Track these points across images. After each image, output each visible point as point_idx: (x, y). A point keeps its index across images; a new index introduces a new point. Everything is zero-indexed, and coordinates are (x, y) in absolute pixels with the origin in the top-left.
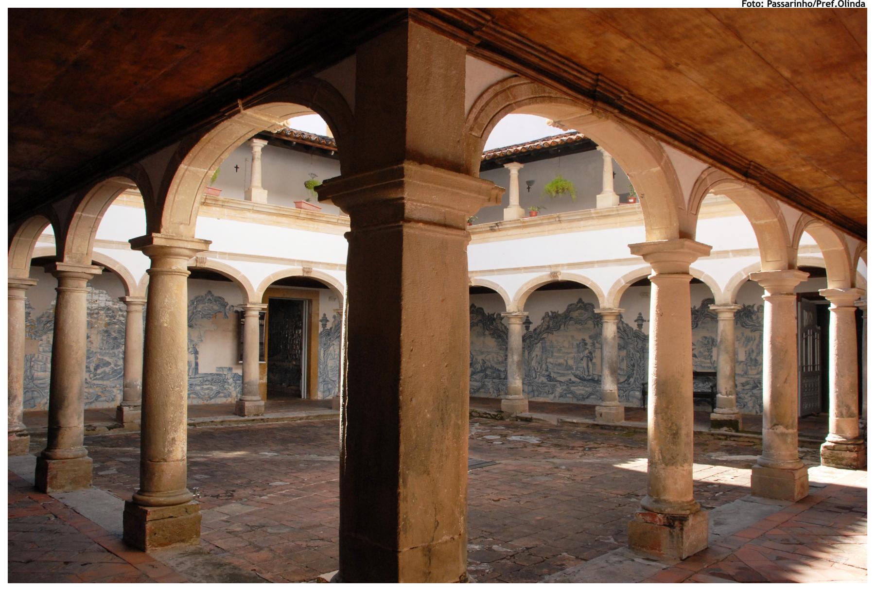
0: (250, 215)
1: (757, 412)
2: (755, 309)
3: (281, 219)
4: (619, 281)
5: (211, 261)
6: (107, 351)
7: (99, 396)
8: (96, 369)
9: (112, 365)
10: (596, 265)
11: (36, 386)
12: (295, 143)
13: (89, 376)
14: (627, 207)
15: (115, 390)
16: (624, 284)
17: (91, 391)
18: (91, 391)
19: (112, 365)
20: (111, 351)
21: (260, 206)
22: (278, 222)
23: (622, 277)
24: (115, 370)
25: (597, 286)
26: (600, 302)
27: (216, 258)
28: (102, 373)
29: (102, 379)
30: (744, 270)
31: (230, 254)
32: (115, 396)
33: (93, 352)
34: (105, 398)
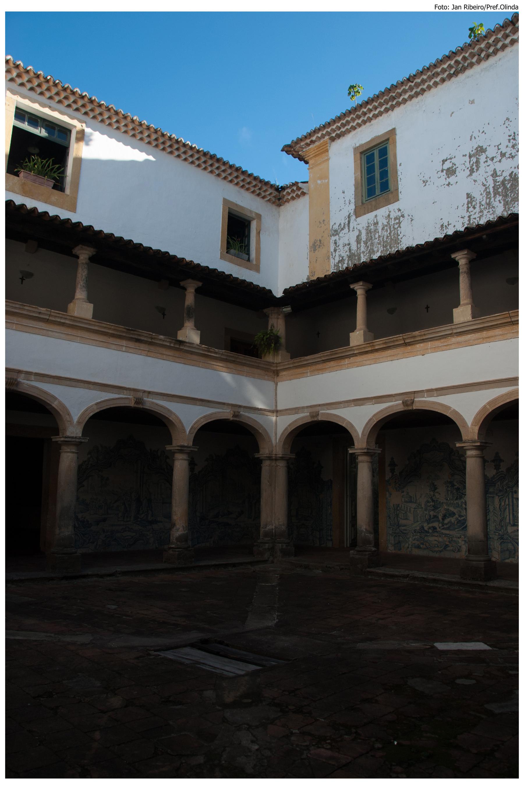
0: (454, 340)
3: (491, 333)
5: (420, 401)
6: (452, 502)
7: (447, 546)
8: (443, 519)
9: (457, 516)
11: (401, 531)
12: (484, 236)
13: (439, 526)
15: (460, 540)
17: (440, 539)
18: (440, 539)
19: (457, 516)
20: (455, 502)
21: (461, 325)
22: (488, 337)
24: (460, 521)
27: (424, 397)
28: (449, 523)
29: (448, 529)
31: (437, 390)
32: (460, 547)
33: (440, 502)
34: (452, 548)
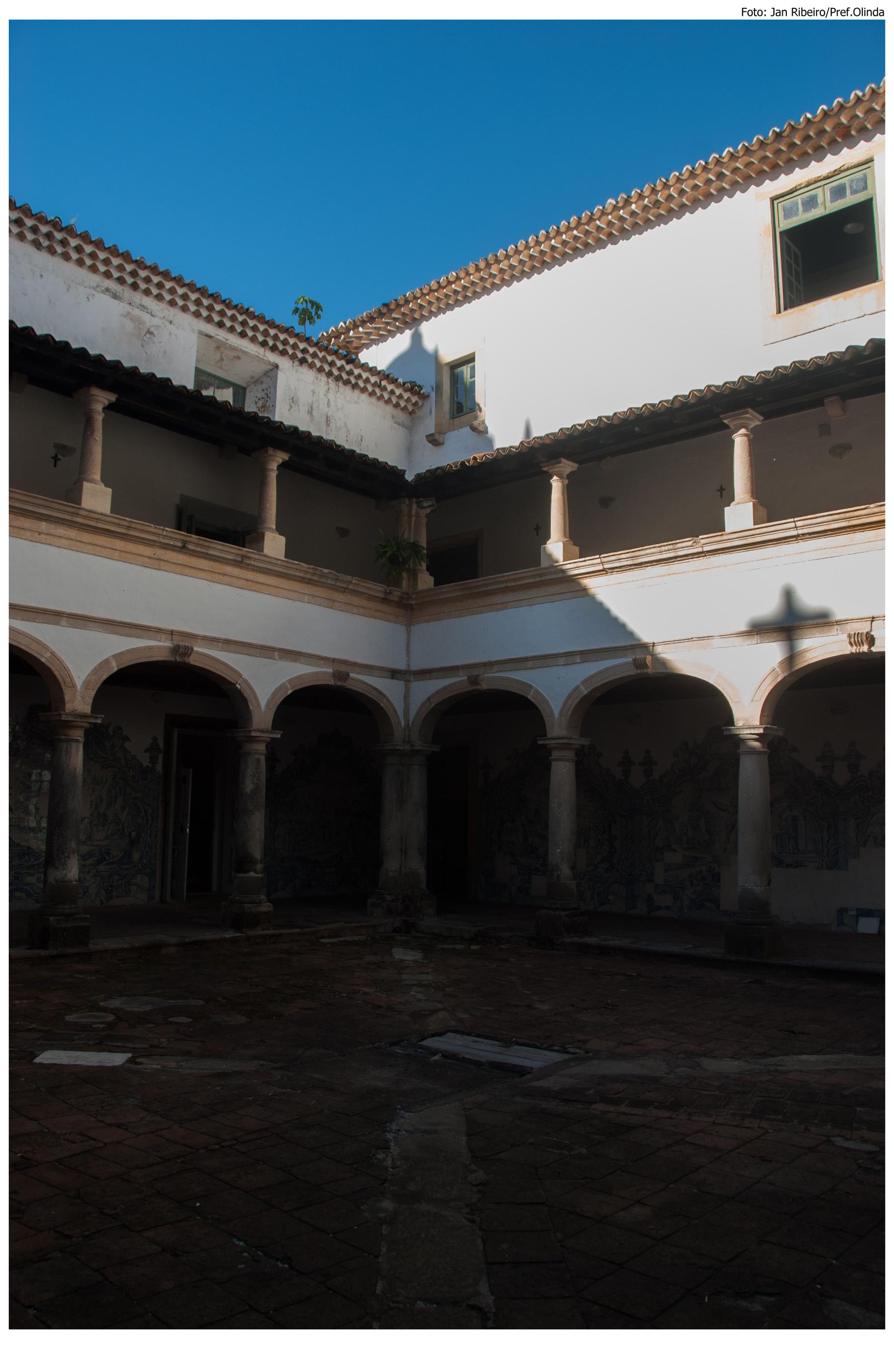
1: (102, 902)
2: (111, 731)
4: (107, 661)
10: (64, 621)
14: (148, 529)
16: (116, 669)
23: (114, 656)
25: (65, 668)
26: (67, 697)
30: (290, 681)
